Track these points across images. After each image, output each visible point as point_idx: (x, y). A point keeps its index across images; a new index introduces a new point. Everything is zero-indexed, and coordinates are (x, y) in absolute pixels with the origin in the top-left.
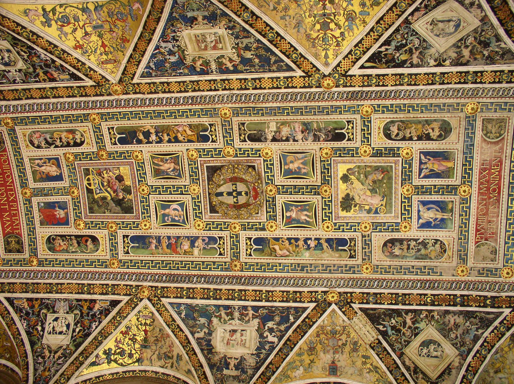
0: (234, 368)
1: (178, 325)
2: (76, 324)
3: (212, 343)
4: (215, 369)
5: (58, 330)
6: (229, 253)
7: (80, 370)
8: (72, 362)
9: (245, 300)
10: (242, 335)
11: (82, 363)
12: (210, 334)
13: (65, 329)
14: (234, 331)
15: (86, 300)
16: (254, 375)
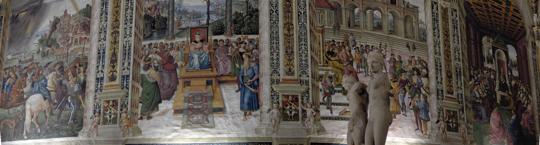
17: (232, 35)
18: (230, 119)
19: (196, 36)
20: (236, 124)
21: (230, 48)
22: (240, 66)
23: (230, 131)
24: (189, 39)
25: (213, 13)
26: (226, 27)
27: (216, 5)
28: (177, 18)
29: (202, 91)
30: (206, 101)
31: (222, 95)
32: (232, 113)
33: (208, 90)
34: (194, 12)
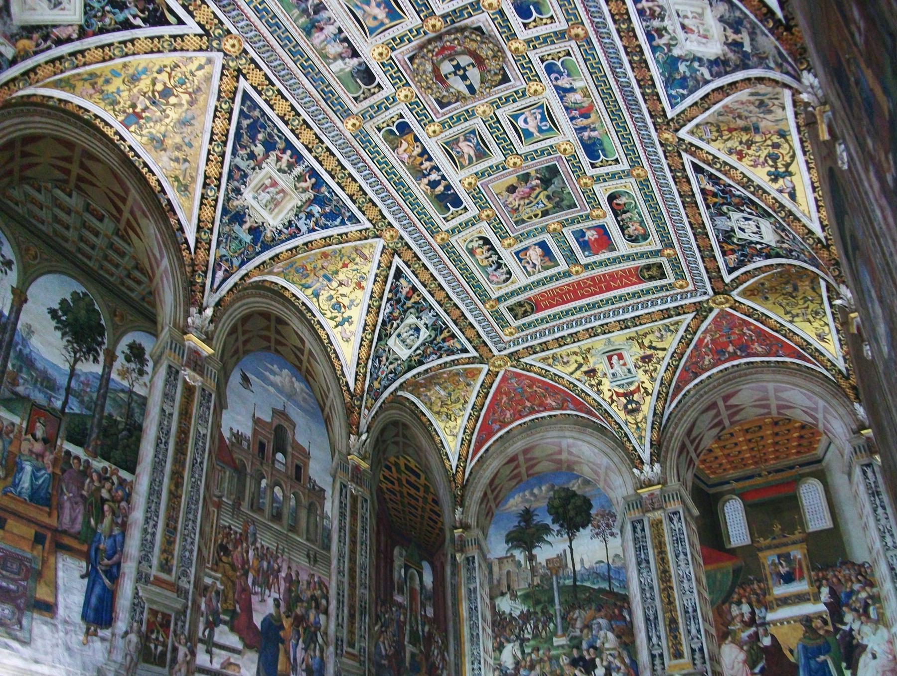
0: (740, 35)
1: (702, 99)
2: (742, 211)
3: (712, 58)
4: (747, 61)
5: (755, 229)
6: (562, 45)
7: (799, 215)
8: (789, 225)
9: (627, 13)
10: (686, 17)
11: (790, 213)
12: (700, 60)
13: (750, 222)
14: (683, 27)
15: (705, 199)
16: (740, 9)
17: (95, 456)
18: (61, 634)
19: (38, 424)
20: (68, 649)
21: (88, 480)
22: (96, 524)
23: (56, 660)
24: (24, 425)
25: (79, 396)
26: (90, 436)
27: (83, 383)
28: (13, 365)
29: (24, 551)
30: (26, 579)
31: (56, 574)
32: (66, 622)
33: (35, 553)
34: (45, 372)
